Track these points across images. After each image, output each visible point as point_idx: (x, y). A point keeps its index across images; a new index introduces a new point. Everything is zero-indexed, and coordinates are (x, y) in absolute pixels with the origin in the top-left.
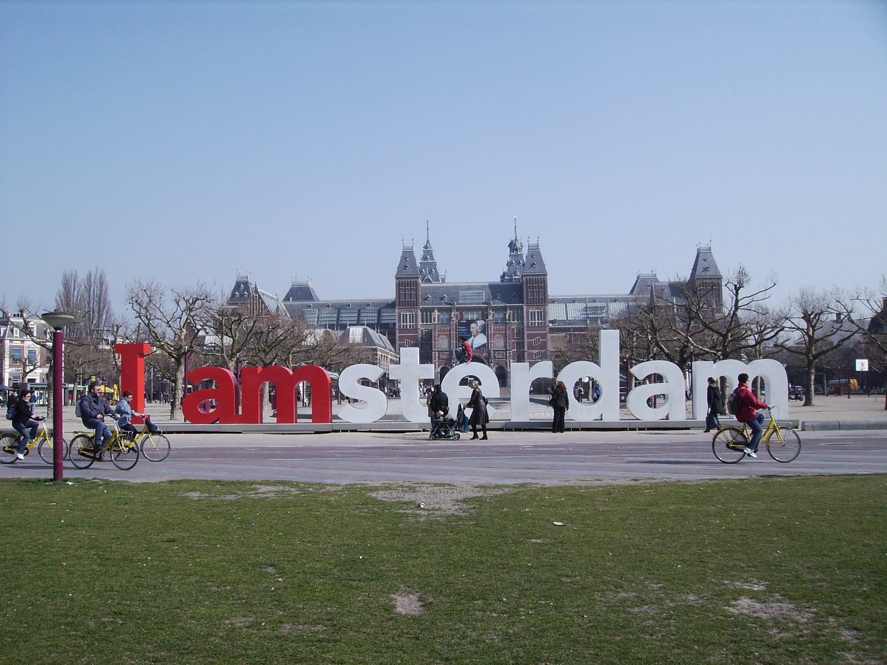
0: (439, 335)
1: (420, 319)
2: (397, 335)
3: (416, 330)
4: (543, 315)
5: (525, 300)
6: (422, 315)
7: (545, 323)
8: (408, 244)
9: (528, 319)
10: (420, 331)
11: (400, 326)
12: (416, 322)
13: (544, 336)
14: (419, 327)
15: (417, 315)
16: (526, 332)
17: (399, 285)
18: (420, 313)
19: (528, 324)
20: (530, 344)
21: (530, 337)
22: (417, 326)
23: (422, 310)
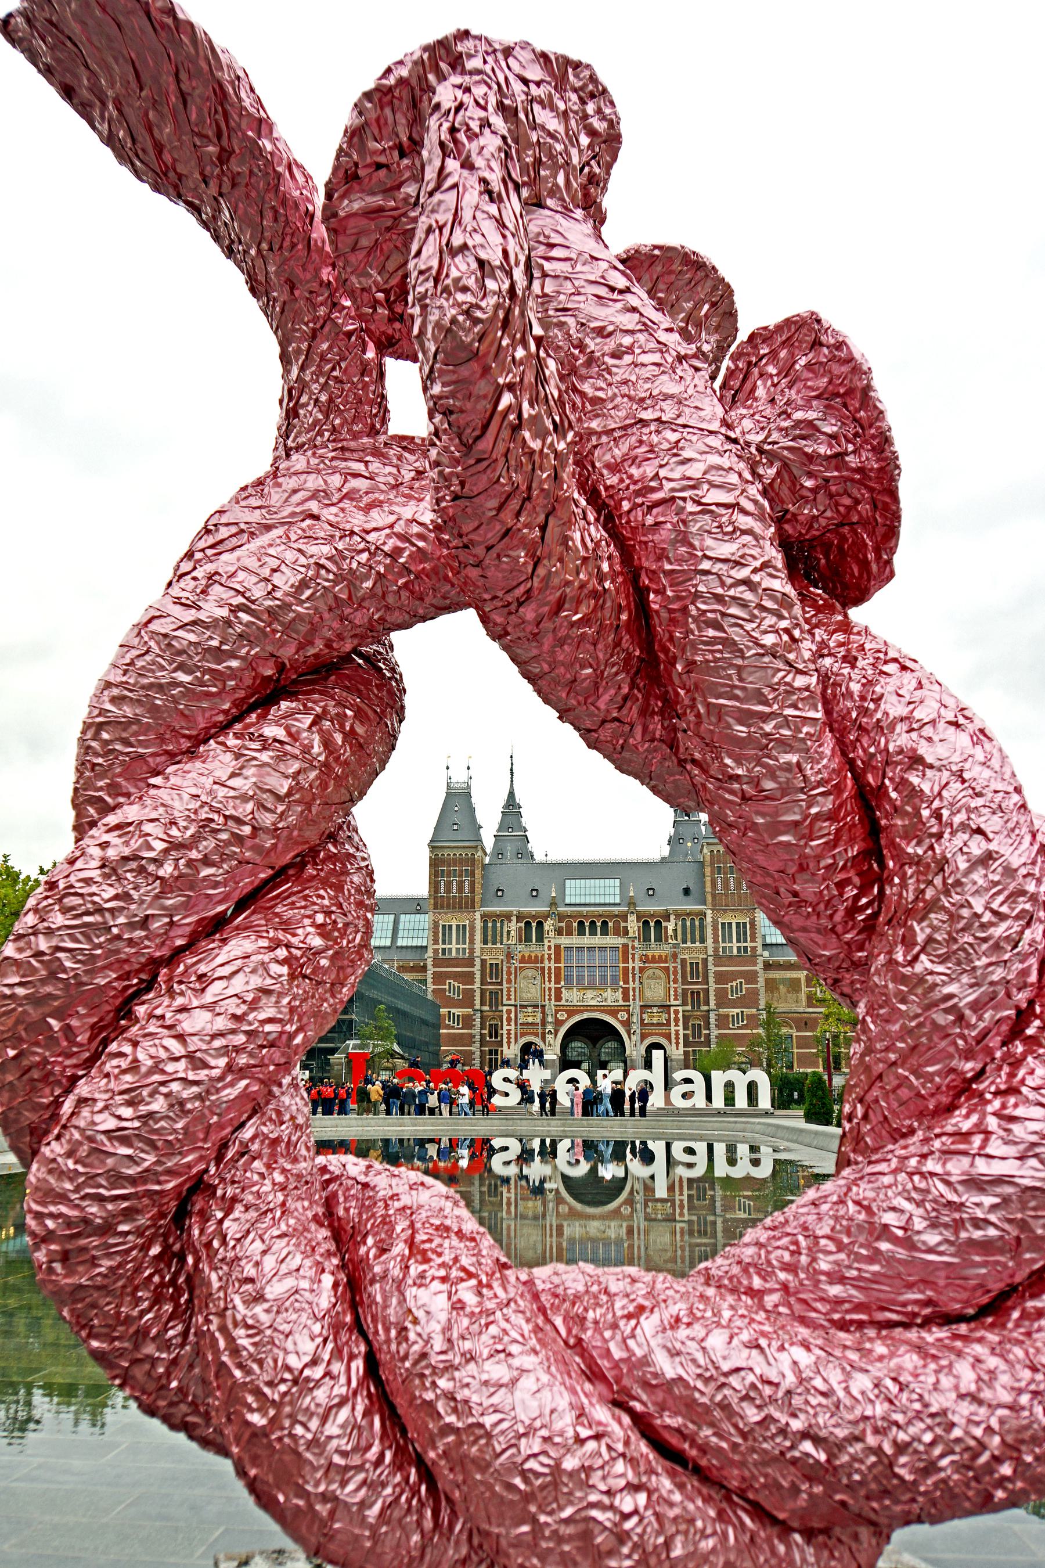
1: (478, 937)
2: (431, 970)
6: (485, 928)
7: (754, 949)
8: (459, 777)
9: (716, 941)
10: (478, 962)
11: (436, 951)
13: (751, 977)
14: (477, 953)
15: (472, 927)
16: (712, 968)
17: (435, 863)
18: (479, 924)
20: (721, 995)
21: (721, 978)
22: (472, 950)
23: (485, 917)
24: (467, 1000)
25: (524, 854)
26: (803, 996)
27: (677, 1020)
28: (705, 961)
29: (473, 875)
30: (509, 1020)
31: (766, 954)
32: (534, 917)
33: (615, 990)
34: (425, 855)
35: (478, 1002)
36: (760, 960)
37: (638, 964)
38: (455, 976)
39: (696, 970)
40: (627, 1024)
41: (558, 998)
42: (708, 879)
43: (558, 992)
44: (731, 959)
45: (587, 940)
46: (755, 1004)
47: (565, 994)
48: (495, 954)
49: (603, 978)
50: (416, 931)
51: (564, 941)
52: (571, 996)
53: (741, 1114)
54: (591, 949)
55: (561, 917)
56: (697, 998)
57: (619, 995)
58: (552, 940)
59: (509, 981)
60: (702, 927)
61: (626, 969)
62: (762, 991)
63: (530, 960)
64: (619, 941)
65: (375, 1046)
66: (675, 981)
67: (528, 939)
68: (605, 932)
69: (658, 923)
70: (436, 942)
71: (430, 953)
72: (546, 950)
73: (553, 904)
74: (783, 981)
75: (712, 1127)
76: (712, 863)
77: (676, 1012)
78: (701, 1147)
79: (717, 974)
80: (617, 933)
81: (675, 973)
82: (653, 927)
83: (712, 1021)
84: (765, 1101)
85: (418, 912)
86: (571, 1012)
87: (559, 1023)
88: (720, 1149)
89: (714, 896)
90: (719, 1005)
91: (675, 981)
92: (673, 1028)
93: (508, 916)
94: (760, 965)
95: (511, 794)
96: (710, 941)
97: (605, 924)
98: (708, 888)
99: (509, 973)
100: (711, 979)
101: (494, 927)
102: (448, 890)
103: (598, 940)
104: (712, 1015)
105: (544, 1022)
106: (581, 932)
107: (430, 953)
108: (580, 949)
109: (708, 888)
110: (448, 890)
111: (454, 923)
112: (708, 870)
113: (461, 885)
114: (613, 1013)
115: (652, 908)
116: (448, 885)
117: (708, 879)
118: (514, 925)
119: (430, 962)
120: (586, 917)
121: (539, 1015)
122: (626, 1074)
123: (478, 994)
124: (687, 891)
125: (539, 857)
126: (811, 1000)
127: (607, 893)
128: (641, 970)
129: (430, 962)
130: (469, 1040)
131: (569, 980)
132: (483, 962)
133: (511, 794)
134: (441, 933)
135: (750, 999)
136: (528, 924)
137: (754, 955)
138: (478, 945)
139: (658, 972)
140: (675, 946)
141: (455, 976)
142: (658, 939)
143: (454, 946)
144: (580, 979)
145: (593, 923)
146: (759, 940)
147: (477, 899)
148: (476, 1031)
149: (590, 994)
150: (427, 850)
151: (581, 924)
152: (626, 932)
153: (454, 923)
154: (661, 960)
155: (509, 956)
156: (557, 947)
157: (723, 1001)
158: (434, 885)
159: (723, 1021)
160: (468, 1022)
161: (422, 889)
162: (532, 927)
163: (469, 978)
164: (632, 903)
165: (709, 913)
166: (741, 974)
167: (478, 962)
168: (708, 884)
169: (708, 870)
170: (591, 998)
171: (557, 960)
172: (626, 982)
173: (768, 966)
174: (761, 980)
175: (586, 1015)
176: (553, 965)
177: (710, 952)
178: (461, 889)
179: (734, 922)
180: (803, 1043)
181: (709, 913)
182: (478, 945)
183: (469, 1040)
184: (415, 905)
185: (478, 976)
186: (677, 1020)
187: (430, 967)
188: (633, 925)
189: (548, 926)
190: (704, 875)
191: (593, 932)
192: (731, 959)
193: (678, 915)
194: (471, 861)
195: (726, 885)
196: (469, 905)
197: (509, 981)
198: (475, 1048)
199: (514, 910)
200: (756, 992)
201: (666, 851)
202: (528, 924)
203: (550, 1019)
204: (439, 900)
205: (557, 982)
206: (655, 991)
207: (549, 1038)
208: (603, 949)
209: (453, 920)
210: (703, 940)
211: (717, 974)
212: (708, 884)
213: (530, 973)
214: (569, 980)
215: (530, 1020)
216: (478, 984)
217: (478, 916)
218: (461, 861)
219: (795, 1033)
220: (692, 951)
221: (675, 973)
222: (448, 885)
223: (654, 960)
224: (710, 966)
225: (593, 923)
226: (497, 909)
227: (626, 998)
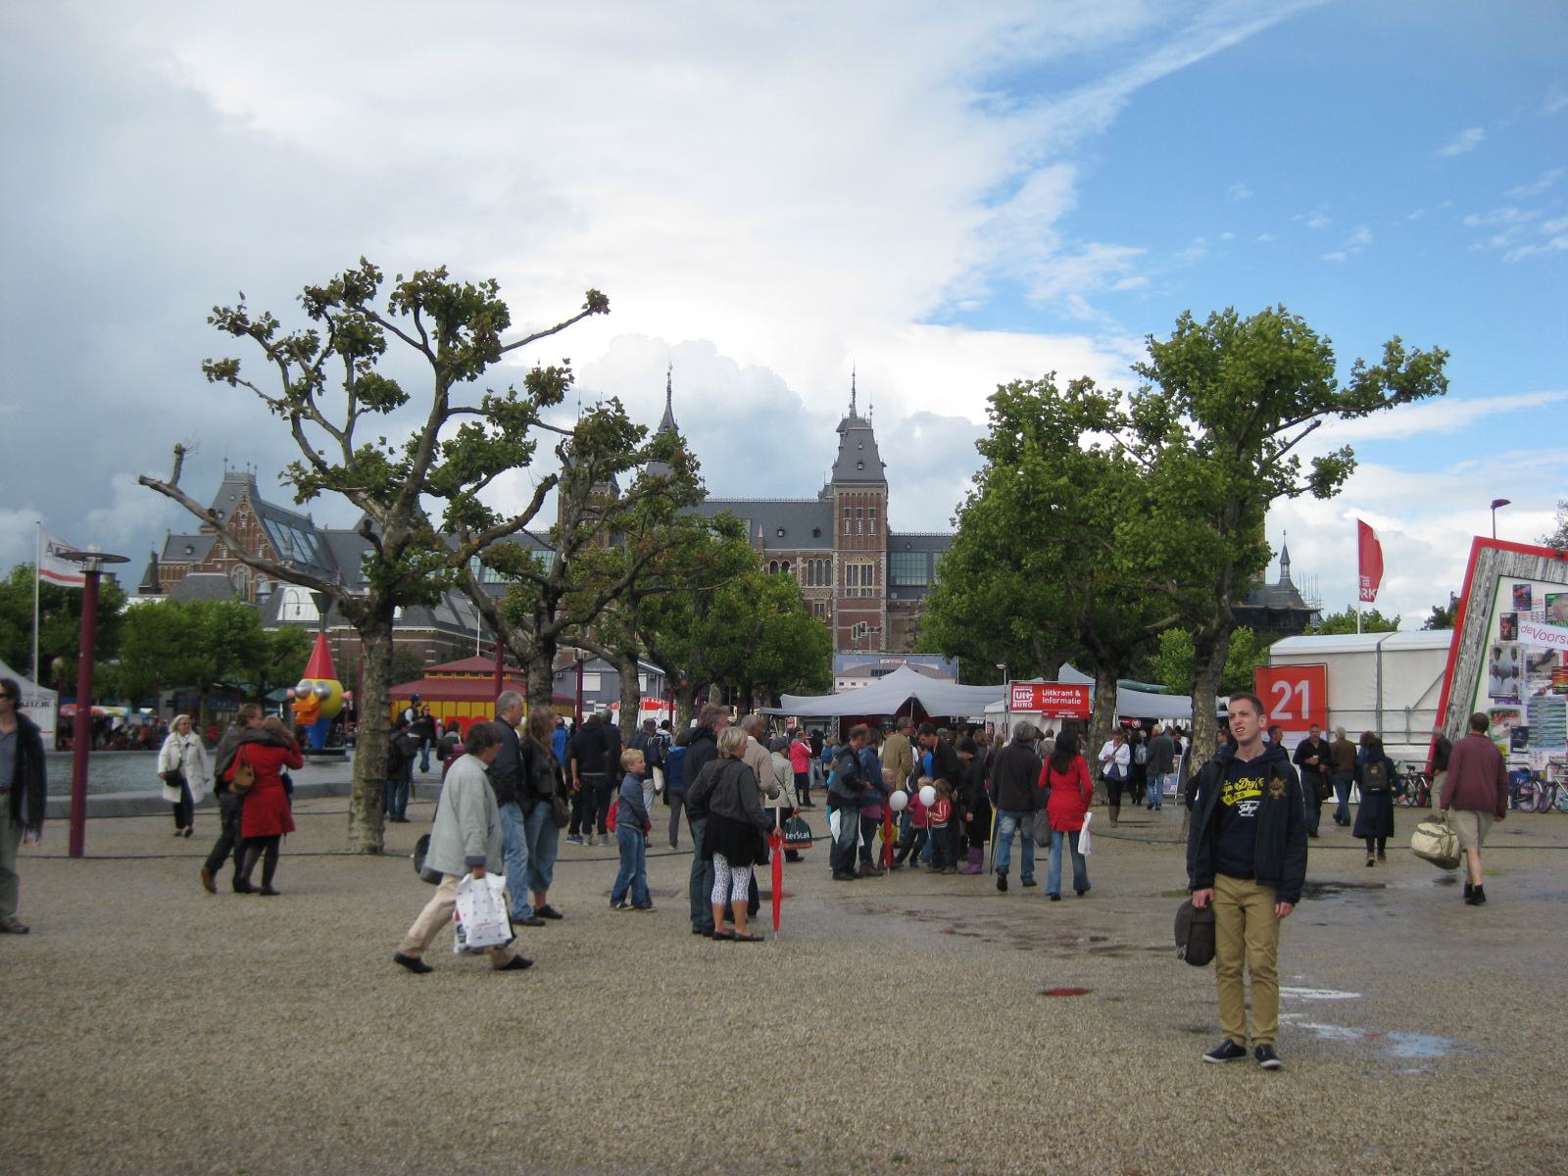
5: (836, 539)
7: (878, 592)
9: (841, 582)
19: (841, 593)
21: (845, 619)
42: (836, 522)
44: (857, 603)
94: (883, 608)
96: (835, 583)
98: (836, 531)
109: (836, 531)
112: (836, 513)
115: (779, 551)
117: (836, 522)
124: (817, 533)
146: (884, 583)
165: (836, 555)
166: (865, 616)
168: (836, 526)
169: (836, 513)
177: (836, 592)
179: (859, 565)
181: (836, 555)
192: (857, 603)
210: (828, 582)
212: (836, 526)
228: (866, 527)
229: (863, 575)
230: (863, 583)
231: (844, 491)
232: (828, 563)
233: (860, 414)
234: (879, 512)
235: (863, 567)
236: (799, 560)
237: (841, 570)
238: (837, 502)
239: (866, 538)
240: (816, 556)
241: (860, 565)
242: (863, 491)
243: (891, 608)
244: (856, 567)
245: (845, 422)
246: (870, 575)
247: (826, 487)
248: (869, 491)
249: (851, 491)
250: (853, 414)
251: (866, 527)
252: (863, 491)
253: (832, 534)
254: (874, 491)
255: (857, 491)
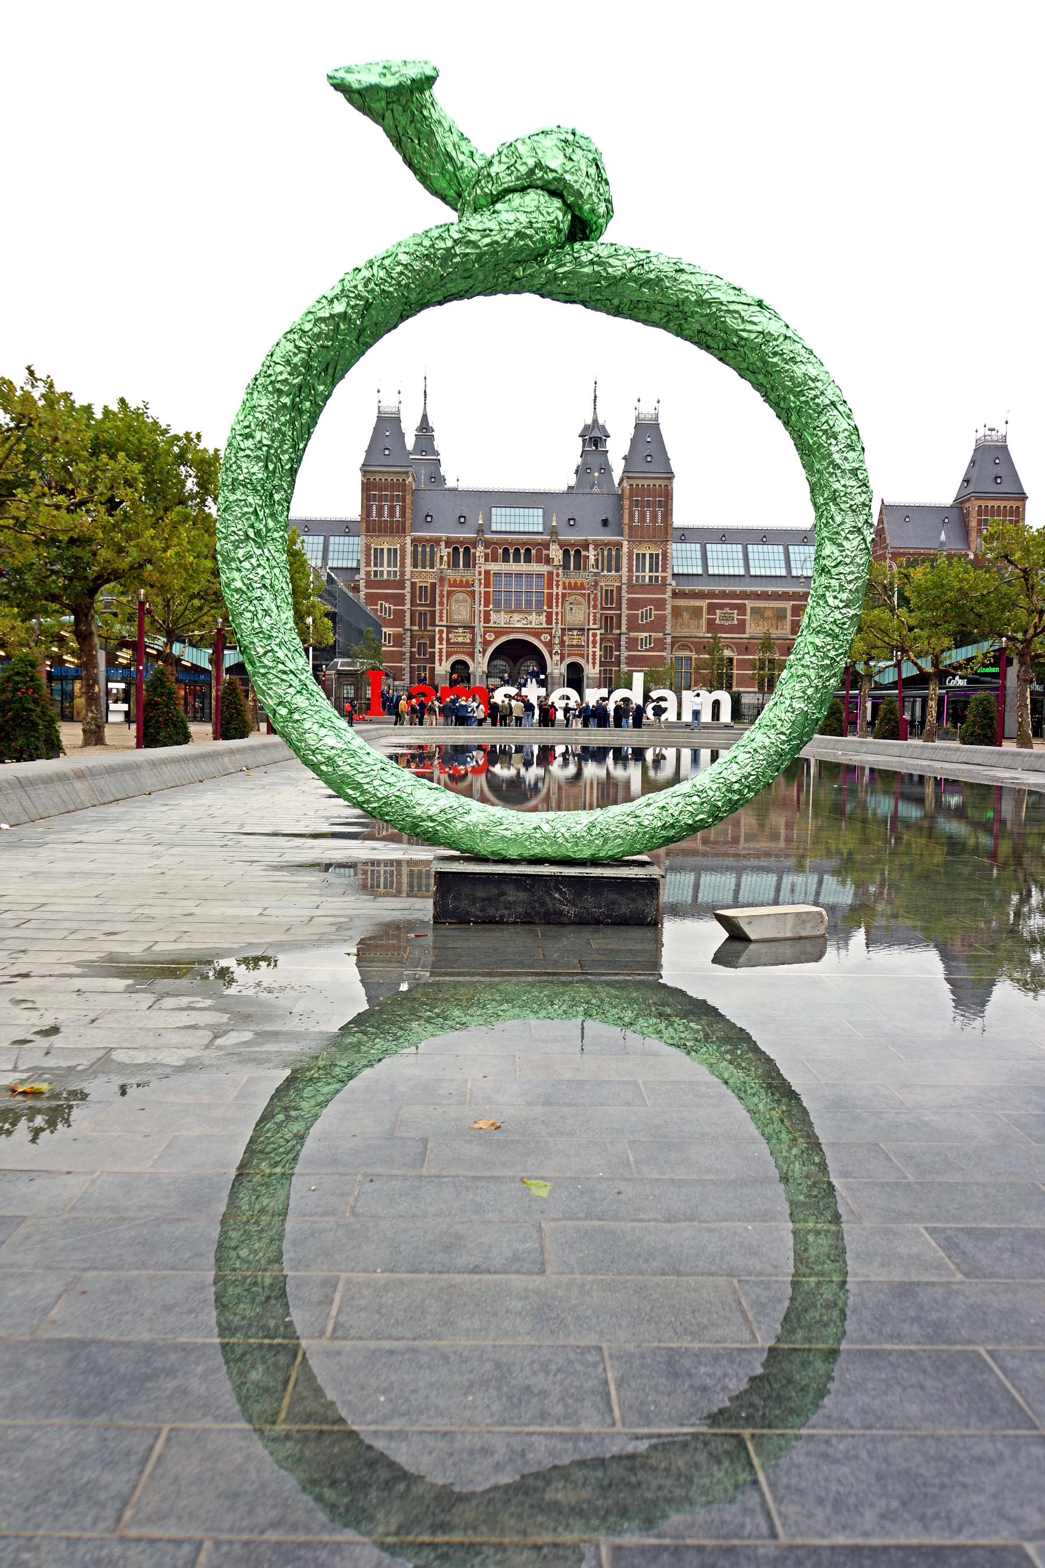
0: (449, 593)
1: (408, 560)
3: (401, 584)
4: (660, 561)
6: (415, 553)
7: (664, 578)
9: (630, 570)
10: (408, 584)
11: (368, 573)
12: (403, 565)
13: (660, 604)
14: (408, 576)
17: (367, 487)
18: (409, 549)
19: (630, 578)
20: (632, 621)
21: (633, 604)
22: (403, 573)
23: (415, 542)
24: (398, 620)
25: (437, 478)
26: (704, 622)
27: (594, 642)
28: (619, 588)
29: (404, 500)
30: (441, 639)
31: (674, 583)
32: (461, 543)
33: (539, 614)
34: (357, 479)
35: (408, 622)
36: (669, 589)
37: (560, 591)
38: (386, 597)
39: (612, 597)
40: (549, 645)
41: (487, 620)
42: (626, 511)
43: (487, 614)
45: (512, 567)
46: (662, 629)
47: (493, 617)
48: (426, 577)
49: (529, 603)
50: (346, 552)
51: (494, 567)
52: (499, 619)
53: (706, 726)
54: (519, 575)
55: (487, 544)
56: (609, 622)
57: (543, 618)
58: (482, 566)
59: (441, 604)
60: (618, 557)
61: (550, 595)
62: (669, 617)
63: (461, 584)
64: (543, 569)
65: (362, 664)
66: (595, 607)
67: (456, 564)
68: (528, 560)
69: (578, 552)
70: (368, 564)
71: (362, 575)
72: (476, 575)
73: (480, 530)
74: (687, 608)
75: (681, 736)
76: (631, 496)
77: (595, 635)
78: (670, 753)
79: (629, 599)
80: (539, 561)
81: (595, 599)
82: (574, 555)
83: (623, 643)
84: (726, 716)
85: (347, 534)
86: (499, 633)
87: (486, 643)
88: (686, 754)
89: (631, 528)
90: (630, 629)
91: (595, 607)
92: (591, 650)
93: (437, 541)
94: (669, 594)
95: (425, 417)
97: (528, 551)
98: (626, 521)
99: (442, 596)
100: (624, 606)
101: (424, 552)
102: (380, 513)
103: (523, 567)
104: (623, 638)
105: (473, 643)
106: (506, 560)
107: (362, 575)
108: (509, 575)
109: (626, 521)
110: (380, 513)
111: (385, 547)
112: (626, 503)
113: (392, 510)
114: (537, 634)
115: (573, 538)
116: (380, 510)
117: (626, 511)
118: (445, 551)
119: (362, 583)
120: (511, 544)
121: (469, 636)
122: (610, 693)
123: (408, 615)
124: (605, 523)
125: (450, 483)
126: (711, 625)
127: (529, 522)
128: (564, 595)
129: (362, 583)
130: (399, 657)
131: (497, 603)
132: (413, 584)
133: (425, 417)
134: (373, 555)
135: (658, 625)
136: (456, 549)
137: (664, 584)
138: (409, 568)
139: (579, 598)
140: (595, 574)
141: (386, 597)
142: (577, 567)
143: (385, 569)
144: (508, 602)
145: (517, 550)
147: (408, 524)
148: (406, 649)
149: (516, 617)
150: (360, 474)
151: (506, 550)
152: (548, 561)
153: (385, 547)
154: (582, 587)
155: (442, 579)
156: (487, 572)
157: (633, 626)
158: (366, 509)
159: (632, 644)
160: (398, 640)
161: (351, 508)
162: (462, 553)
163: (399, 599)
164: (554, 532)
165: (625, 543)
166: (651, 601)
167: (408, 584)
168: (626, 516)
169: (626, 503)
170: (517, 621)
171: (487, 585)
172: (550, 606)
173: (675, 595)
174: (669, 607)
175: (512, 637)
176: (482, 590)
177: (625, 580)
178: (392, 513)
179: (648, 553)
180: (743, 664)
181: (625, 543)
182: (409, 568)
183: (399, 657)
184: (345, 528)
185: (408, 597)
186: (594, 642)
187: (362, 588)
188: (556, 553)
189: (480, 551)
190: (621, 507)
191: (517, 560)
192: (643, 588)
193: (597, 545)
194: (403, 486)
195: (642, 518)
196: (399, 529)
197: (441, 604)
198: (405, 665)
199: (444, 535)
200: (663, 618)
201: (573, 480)
202: (456, 549)
203: (479, 640)
204: (371, 524)
205: (486, 605)
206: (578, 614)
207: (478, 656)
208: (529, 575)
209: (385, 544)
210: (618, 570)
211: (629, 599)
212: (626, 516)
213: (461, 596)
214: (497, 603)
215: (460, 640)
216: (408, 606)
217: (408, 540)
218: (393, 486)
219: (694, 656)
220: (609, 580)
221: (595, 599)
222: (380, 510)
223: (576, 587)
224: (624, 593)
225: (517, 550)
226: (427, 535)
227: (549, 621)
228: (654, 516)
229: (651, 564)
230: (651, 571)
231: (634, 482)
232: (618, 551)
233: (601, 422)
234: (666, 502)
235: (651, 555)
236: (591, 547)
237: (630, 559)
238: (627, 492)
239: (654, 529)
240: (606, 545)
241: (648, 553)
242: (651, 482)
243: (675, 595)
244: (644, 555)
245: (586, 428)
246: (657, 564)
247: (569, 488)
248: (658, 483)
249: (640, 482)
250: (595, 421)
251: (654, 516)
252: (651, 482)
253: (620, 524)
254: (663, 483)
255: (646, 483)
